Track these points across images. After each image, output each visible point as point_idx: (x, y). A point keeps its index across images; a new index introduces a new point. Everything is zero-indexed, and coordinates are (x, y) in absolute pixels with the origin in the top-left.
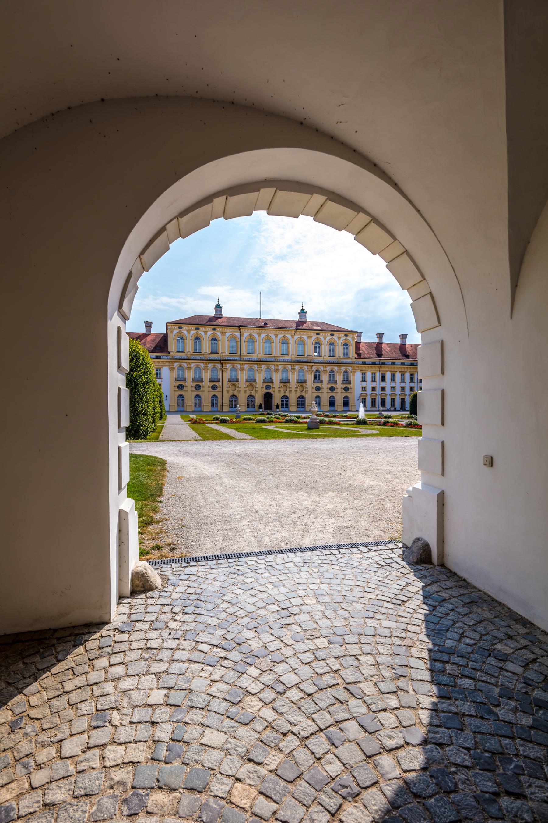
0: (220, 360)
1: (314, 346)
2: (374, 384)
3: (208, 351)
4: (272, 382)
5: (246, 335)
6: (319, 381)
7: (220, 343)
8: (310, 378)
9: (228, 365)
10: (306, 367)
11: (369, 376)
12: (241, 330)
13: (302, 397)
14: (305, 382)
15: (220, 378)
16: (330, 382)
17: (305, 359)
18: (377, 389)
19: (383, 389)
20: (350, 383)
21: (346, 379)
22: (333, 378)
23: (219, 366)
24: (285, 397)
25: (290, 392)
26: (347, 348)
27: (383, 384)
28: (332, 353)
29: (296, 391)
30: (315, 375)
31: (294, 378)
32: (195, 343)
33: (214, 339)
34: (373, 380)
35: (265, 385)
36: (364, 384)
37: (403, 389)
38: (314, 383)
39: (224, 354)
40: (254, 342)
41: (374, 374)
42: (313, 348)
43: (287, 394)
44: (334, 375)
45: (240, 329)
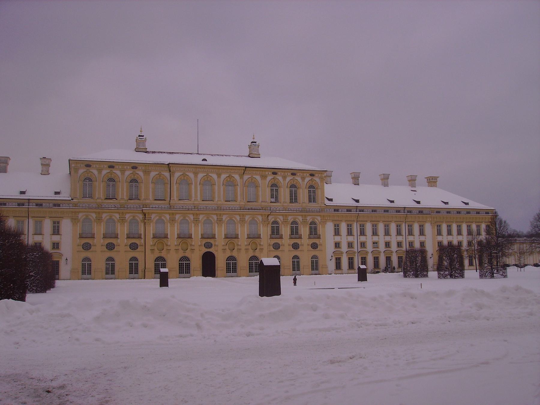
1: (270, 188)
2: (350, 239)
4: (214, 237)
5: (177, 175)
8: (265, 231)
10: (260, 218)
12: (171, 169)
14: (259, 237)
15: (142, 233)
16: (293, 236)
19: (363, 245)
21: (314, 232)
24: (231, 258)
26: (314, 192)
27: (363, 239)
28: (294, 198)
31: (243, 231)
32: (108, 186)
34: (350, 233)
36: (337, 239)
37: (387, 245)
42: (268, 191)
43: (235, 254)
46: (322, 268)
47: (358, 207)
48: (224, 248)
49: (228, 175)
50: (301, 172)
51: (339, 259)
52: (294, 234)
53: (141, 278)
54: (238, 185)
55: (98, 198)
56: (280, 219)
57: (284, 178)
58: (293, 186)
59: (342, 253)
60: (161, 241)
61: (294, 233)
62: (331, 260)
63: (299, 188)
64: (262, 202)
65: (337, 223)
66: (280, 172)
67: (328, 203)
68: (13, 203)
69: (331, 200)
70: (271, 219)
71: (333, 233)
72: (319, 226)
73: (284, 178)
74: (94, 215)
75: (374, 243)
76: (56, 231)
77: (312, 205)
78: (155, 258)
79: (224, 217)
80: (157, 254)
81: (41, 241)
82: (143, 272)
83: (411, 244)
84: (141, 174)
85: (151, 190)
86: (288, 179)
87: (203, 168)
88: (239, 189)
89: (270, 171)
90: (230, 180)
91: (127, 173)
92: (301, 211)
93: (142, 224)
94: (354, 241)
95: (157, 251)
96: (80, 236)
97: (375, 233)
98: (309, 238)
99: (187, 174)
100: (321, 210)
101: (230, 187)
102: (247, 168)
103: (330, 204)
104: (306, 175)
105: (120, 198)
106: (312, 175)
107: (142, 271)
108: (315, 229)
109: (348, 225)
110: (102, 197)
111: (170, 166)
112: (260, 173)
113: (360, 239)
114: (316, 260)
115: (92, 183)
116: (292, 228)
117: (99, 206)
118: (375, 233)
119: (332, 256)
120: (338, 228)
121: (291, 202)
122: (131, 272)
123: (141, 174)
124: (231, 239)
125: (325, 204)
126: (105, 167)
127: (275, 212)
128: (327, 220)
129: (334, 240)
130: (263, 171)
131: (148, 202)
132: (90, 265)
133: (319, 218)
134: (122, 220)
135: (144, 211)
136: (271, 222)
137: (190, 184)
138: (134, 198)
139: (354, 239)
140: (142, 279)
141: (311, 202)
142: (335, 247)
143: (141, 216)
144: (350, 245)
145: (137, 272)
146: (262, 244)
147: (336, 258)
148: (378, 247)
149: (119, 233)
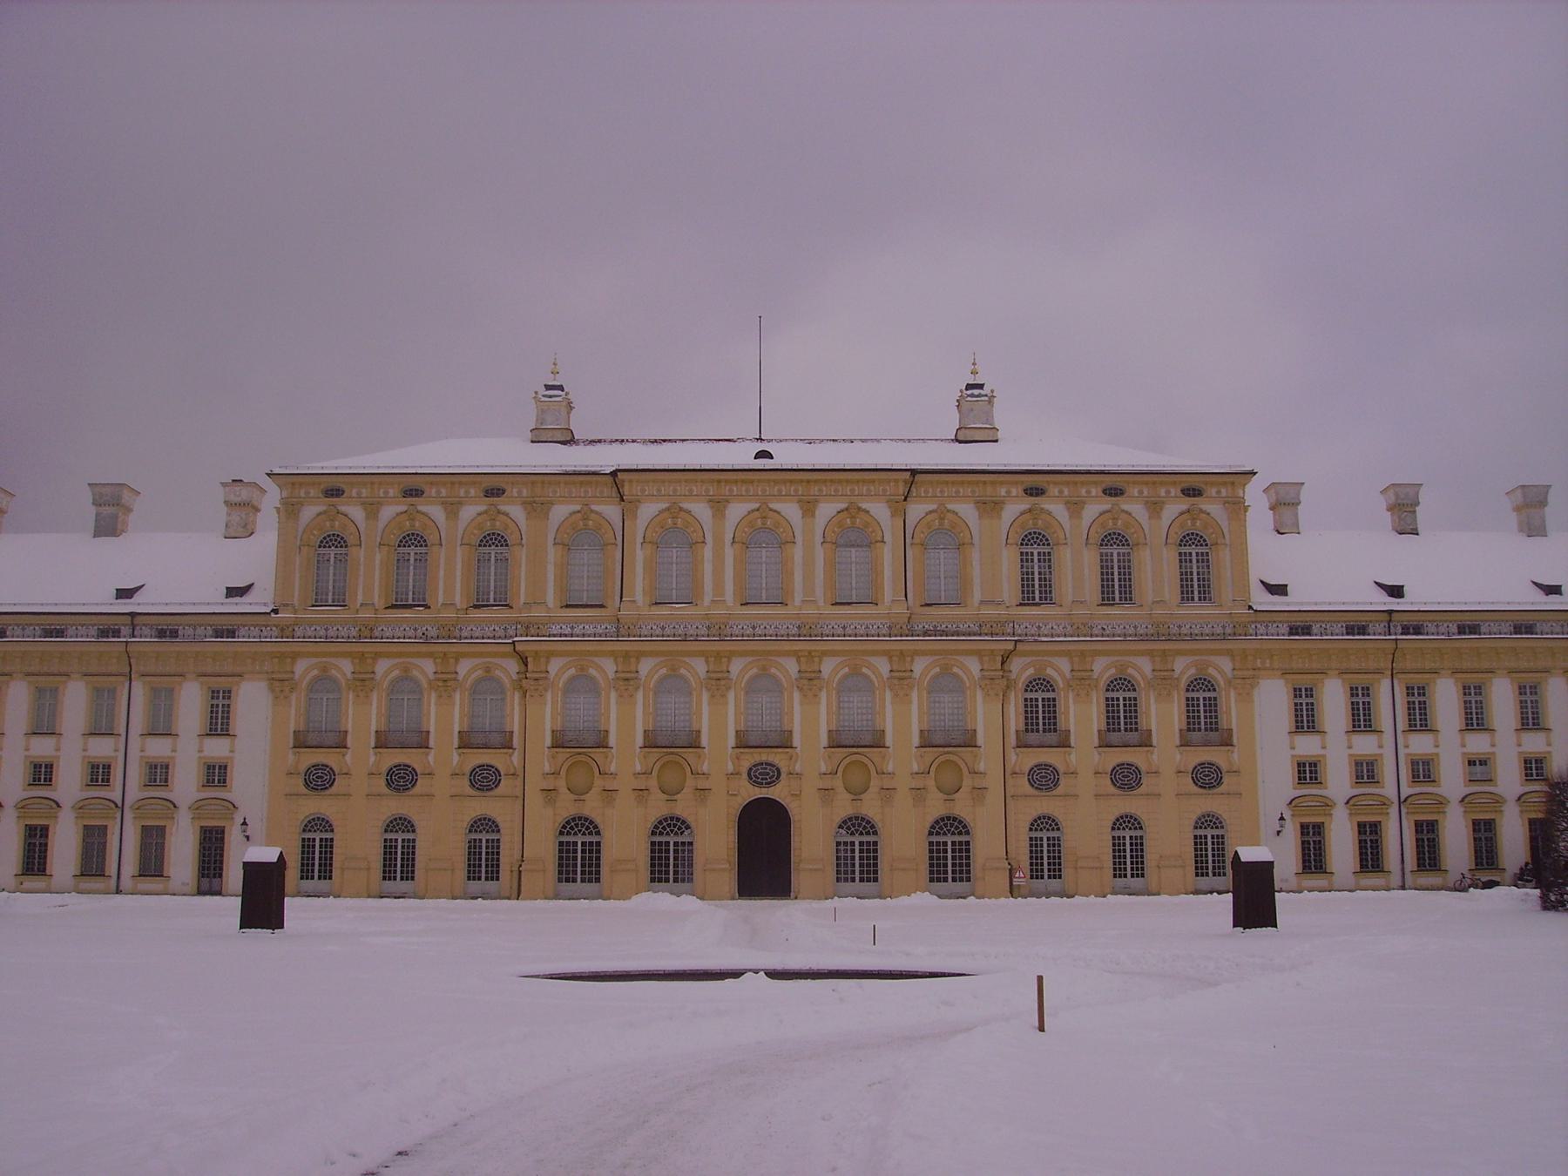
2: (1365, 745)
4: (784, 743)
5: (648, 511)
6: (1133, 737)
7: (522, 556)
9: (554, 666)
10: (974, 665)
11: (1333, 701)
12: (626, 490)
13: (949, 824)
14: (970, 742)
15: (516, 728)
16: (1114, 737)
19: (1423, 770)
20: (1227, 742)
22: (1132, 725)
24: (858, 824)
25: (888, 792)
26: (1204, 559)
27: (1420, 744)
29: (918, 793)
30: (1030, 705)
34: (1362, 719)
35: (750, 758)
36: (1308, 746)
38: (1021, 745)
40: (960, 546)
41: (1366, 691)
43: (870, 807)
44: (1051, 705)
47: (1394, 615)
48: (827, 783)
49: (844, 506)
50: (1147, 483)
51: (1318, 829)
52: (1119, 730)
53: (508, 895)
54: (883, 542)
55: (362, 605)
56: (1059, 669)
57: (1075, 507)
58: (1113, 538)
59: (1327, 805)
60: (952, 757)
61: (1119, 724)
62: (1279, 832)
63: (1138, 544)
64: (982, 602)
65: (1304, 681)
66: (1055, 483)
67: (1263, 600)
68: (79, 628)
69: (1279, 590)
70: (1021, 669)
71: (1285, 719)
72: (1066, 697)
73: (1075, 507)
74: (347, 666)
75: (1471, 763)
76: (219, 723)
77: (1197, 610)
78: (560, 820)
79: (828, 666)
80: (566, 808)
81: (227, 758)
82: (516, 875)
84: (517, 512)
85: (551, 569)
86: (1091, 511)
87: (743, 481)
88: (888, 557)
89: (1016, 483)
90: (853, 523)
91: (469, 512)
92: (1145, 638)
93: (517, 696)
95: (565, 797)
96: (461, 738)
98: (1105, 744)
99: (685, 506)
100: (1237, 630)
101: (853, 550)
103: (1274, 604)
104: (1168, 492)
105: (441, 600)
106: (1192, 492)
107: (512, 871)
108: (1212, 706)
109: (1353, 691)
110: (376, 600)
111: (623, 481)
112: (973, 492)
113: (1407, 747)
114: (1215, 832)
115: (346, 554)
116: (1110, 704)
117: (367, 632)
119: (1282, 818)
120: (1422, 699)
121: (1107, 599)
122: (473, 875)
123: (517, 512)
124: (854, 750)
125: (1250, 607)
126: (391, 493)
127: (1036, 641)
128: (1259, 669)
129: (1351, 752)
130: (985, 483)
131: (537, 613)
132: (328, 845)
133: (1226, 664)
134: (445, 682)
135: (519, 647)
136: (1021, 685)
137: (695, 544)
138: (492, 602)
139: (1381, 747)
140: (509, 898)
141: (1193, 599)
142: (1300, 779)
143: (513, 666)
144: (1365, 771)
145: (494, 875)
146: (981, 767)
147: (1304, 828)
148: (1491, 780)
149: (432, 730)
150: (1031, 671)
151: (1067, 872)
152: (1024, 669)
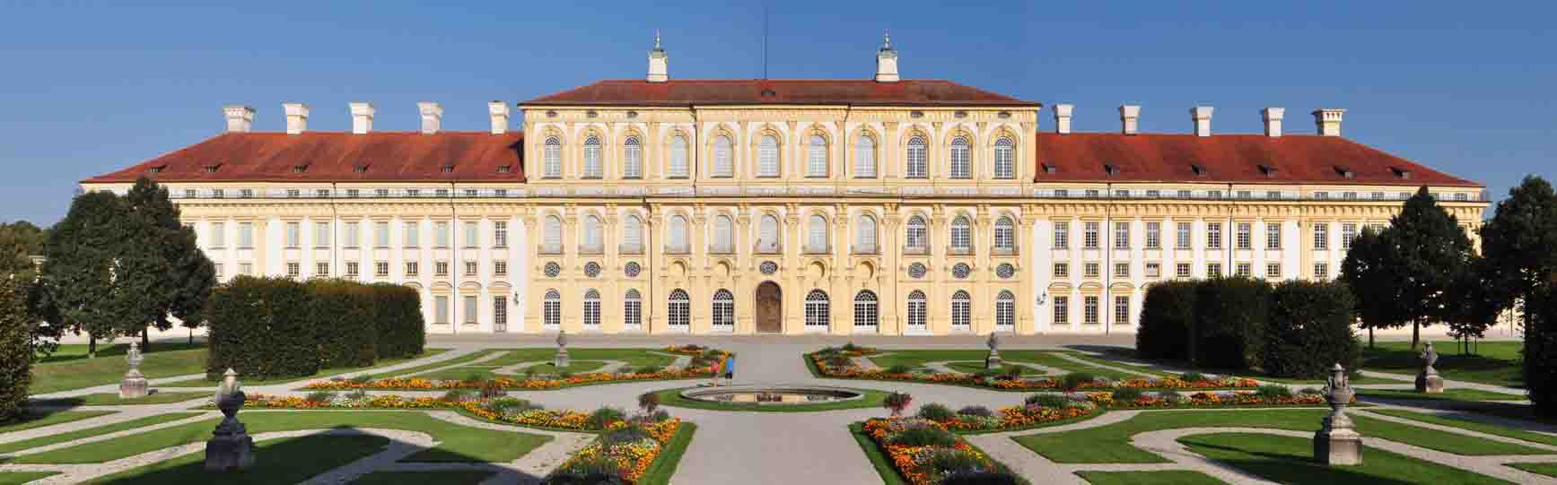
0: (645, 197)
2: (1092, 256)
3: (617, 176)
8: (893, 239)
11: (1077, 232)
13: (867, 294)
17: (880, 190)
18: (1103, 269)
20: (1015, 253)
21: (1006, 237)
23: (643, 211)
27: (1121, 256)
28: (961, 167)
33: (633, 140)
34: (1091, 241)
36: (1061, 256)
39: (655, 180)
45: (694, 111)
46: (1021, 319)
51: (1065, 300)
59: (1070, 287)
71: (1051, 241)
83: (1246, 267)
93: (646, 226)
94: (1100, 262)
97: (1154, 242)
102: (852, 108)
118: (1154, 242)
119: (1044, 295)
131: (655, 180)
136: (906, 221)
144: (1092, 269)
147: (1057, 299)
150: (911, 215)
151: (929, 322)
152: (906, 215)
